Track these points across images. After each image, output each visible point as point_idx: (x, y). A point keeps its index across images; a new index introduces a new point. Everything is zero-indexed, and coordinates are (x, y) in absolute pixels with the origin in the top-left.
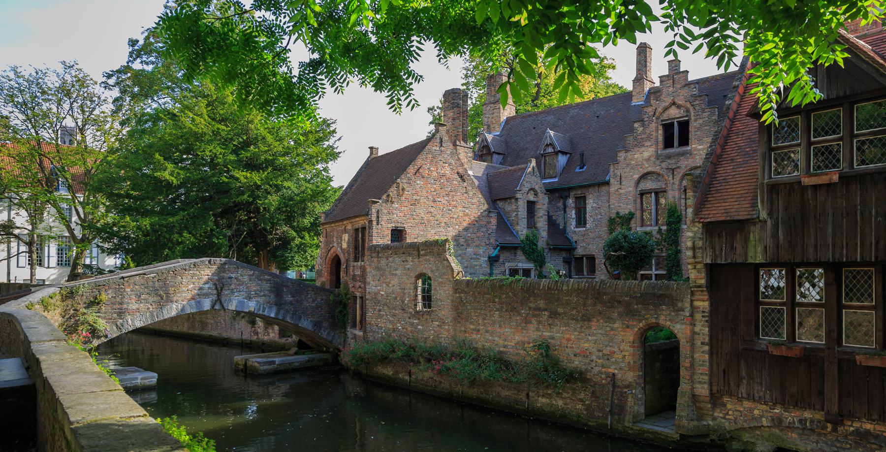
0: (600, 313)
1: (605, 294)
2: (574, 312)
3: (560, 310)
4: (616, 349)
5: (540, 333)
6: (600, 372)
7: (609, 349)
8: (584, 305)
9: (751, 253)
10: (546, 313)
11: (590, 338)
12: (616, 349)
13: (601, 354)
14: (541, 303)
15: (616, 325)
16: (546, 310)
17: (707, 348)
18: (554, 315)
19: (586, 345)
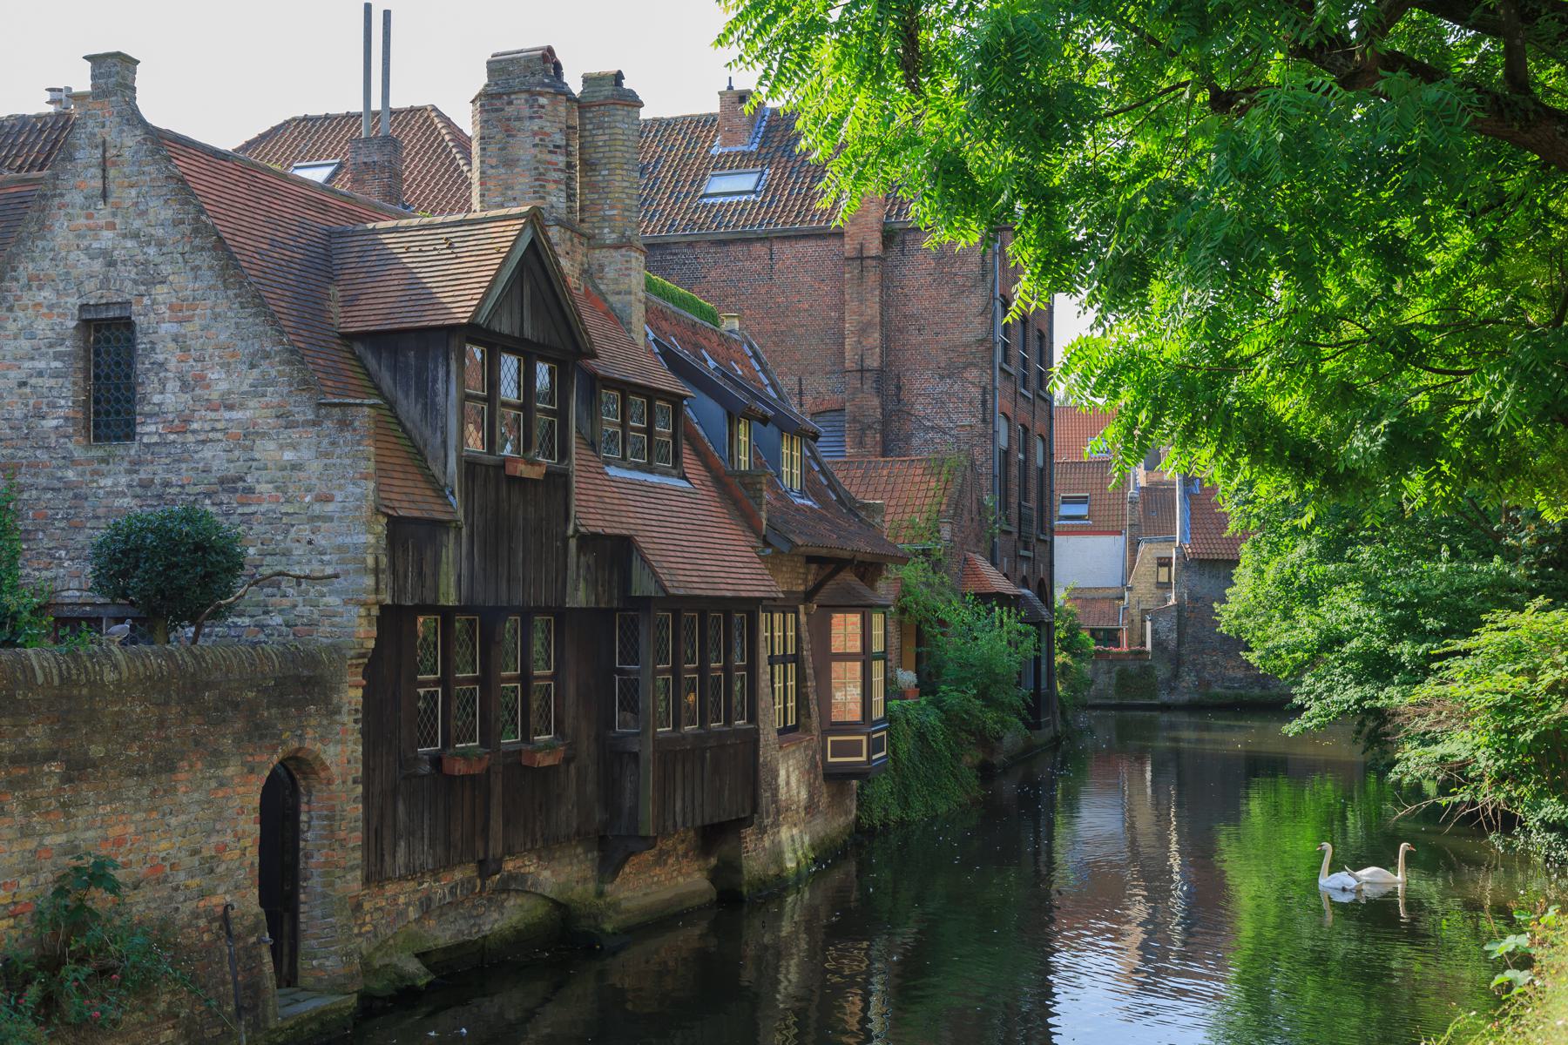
0: (197, 743)
1: (208, 686)
2: (134, 752)
3: (97, 751)
4: (229, 838)
5: (31, 844)
6: (196, 915)
7: (214, 839)
8: (161, 724)
9: (442, 588)
10: (55, 767)
11: (173, 821)
12: (229, 838)
13: (196, 861)
14: (38, 735)
15: (230, 771)
16: (51, 757)
17: (360, 789)
18: (78, 769)
19: (164, 845)
